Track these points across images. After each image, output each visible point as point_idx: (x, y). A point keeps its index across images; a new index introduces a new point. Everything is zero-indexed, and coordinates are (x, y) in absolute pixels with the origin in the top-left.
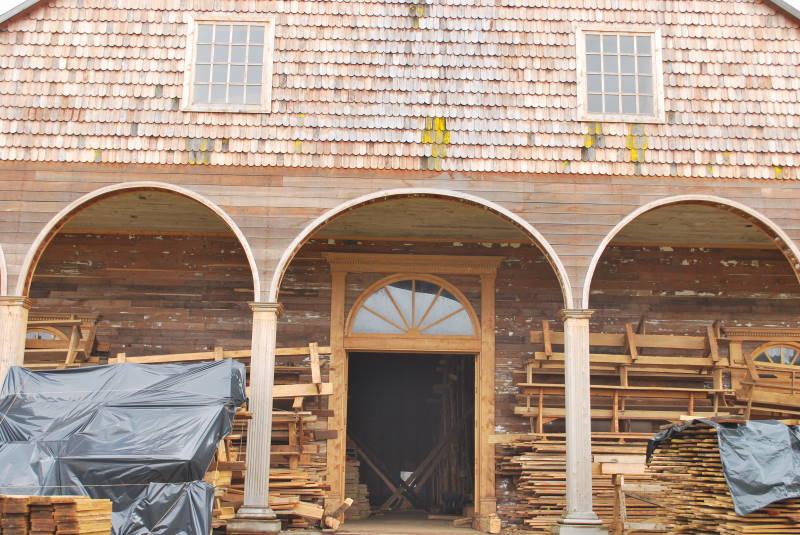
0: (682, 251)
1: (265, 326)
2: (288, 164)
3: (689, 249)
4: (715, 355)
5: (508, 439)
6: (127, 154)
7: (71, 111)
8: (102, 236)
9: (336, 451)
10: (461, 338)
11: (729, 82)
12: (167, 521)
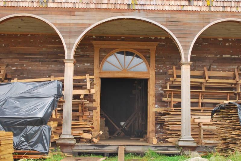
0: (226, 40)
1: (69, 68)
2: (77, 7)
3: (229, 39)
4: (237, 79)
5: (160, 110)
6: (16, 3)
8: (7, 34)
9: (96, 114)
10: (143, 73)
12: (34, 139)
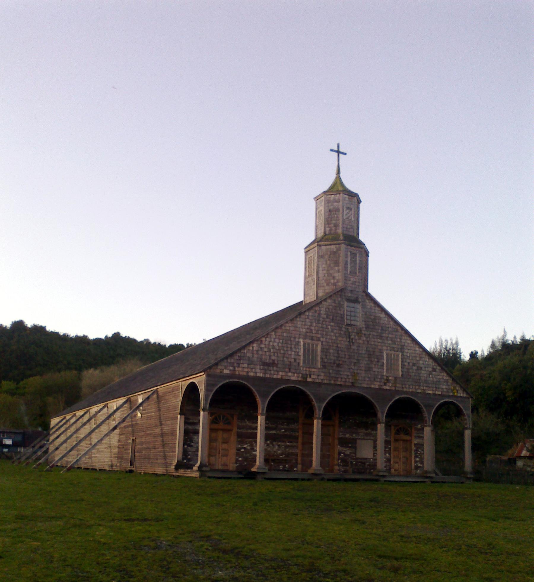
7: (273, 364)
11: (414, 368)
